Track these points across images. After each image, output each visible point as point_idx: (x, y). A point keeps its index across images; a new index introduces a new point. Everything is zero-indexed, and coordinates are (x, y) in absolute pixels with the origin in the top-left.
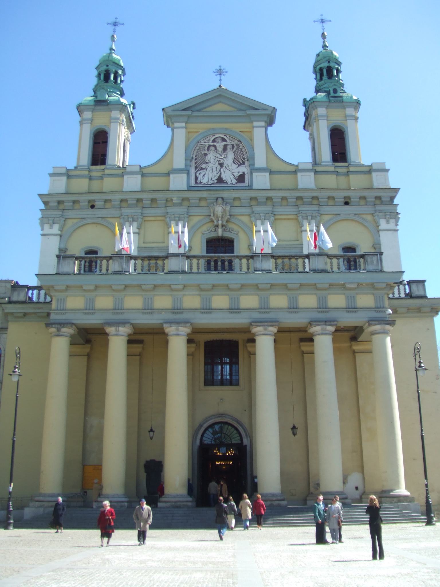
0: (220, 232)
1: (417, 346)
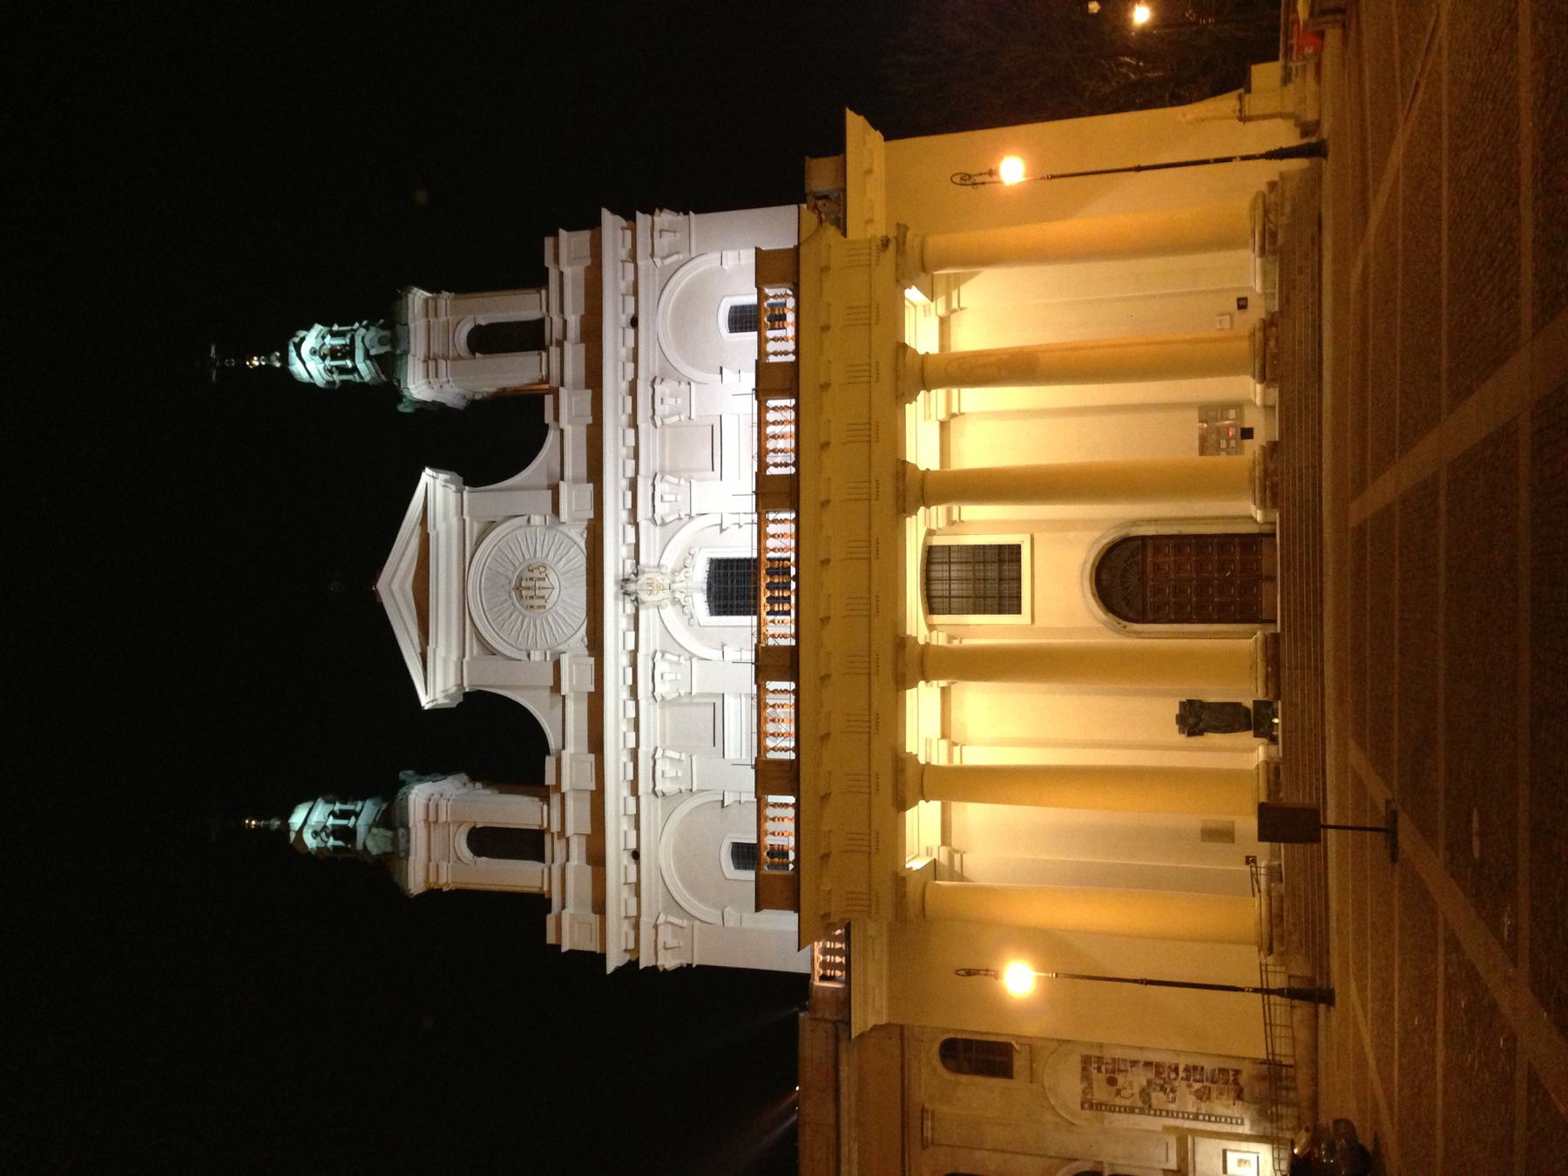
1: (957, 179)
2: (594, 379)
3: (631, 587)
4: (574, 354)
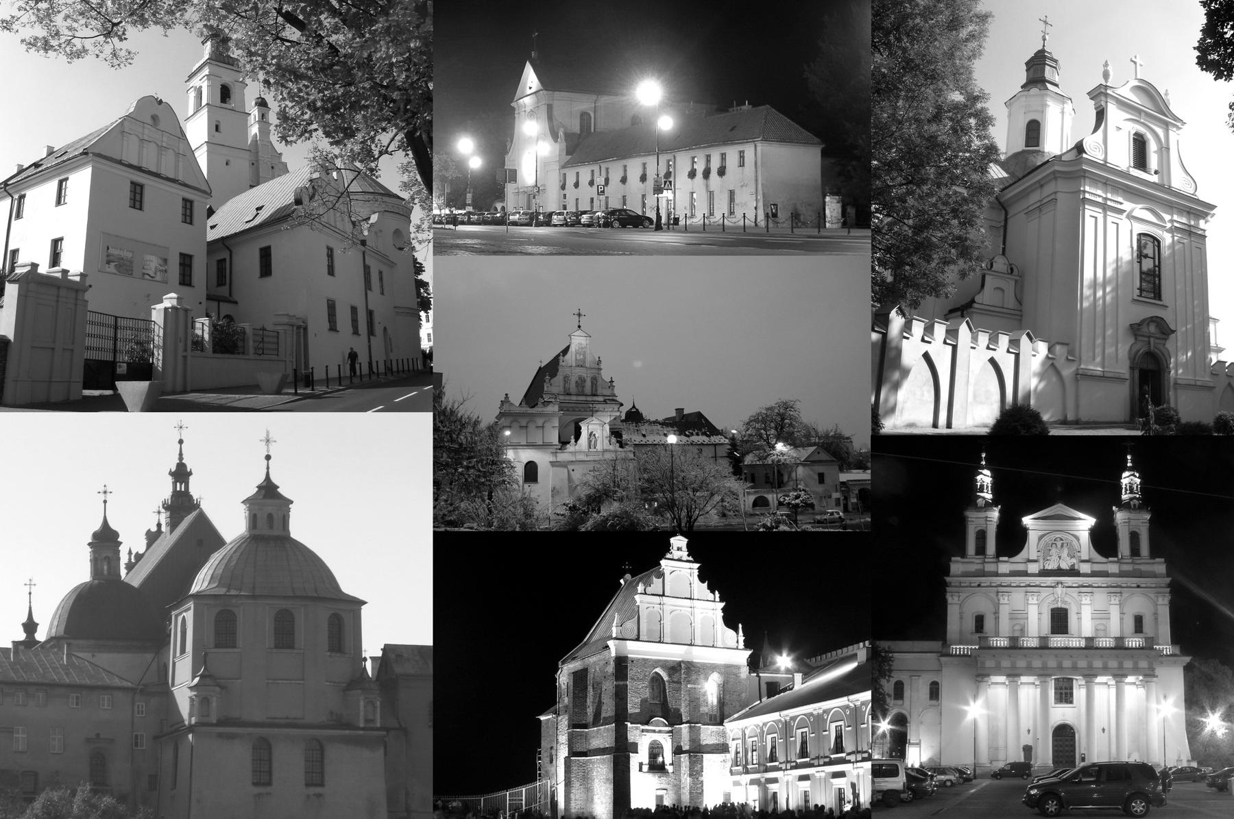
2: (1122, 574)
3: (1060, 585)
4: (1126, 568)
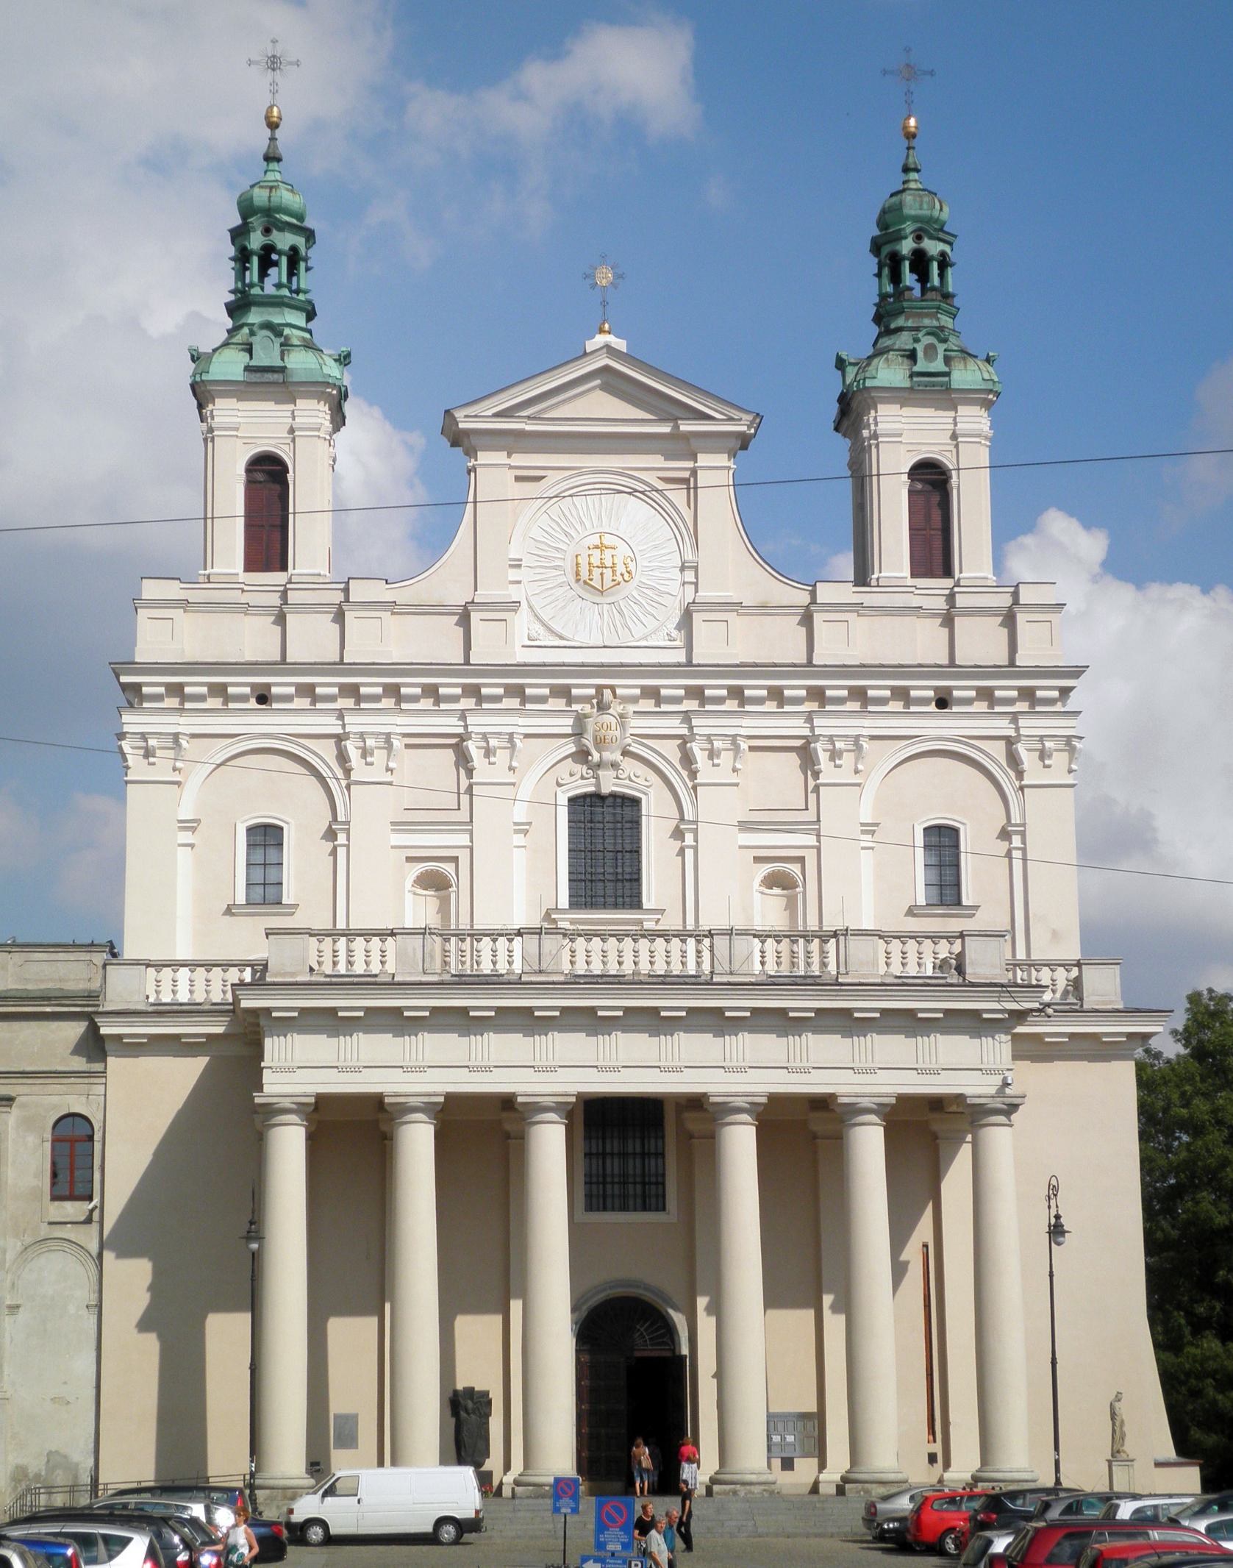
0: (609, 785)
1: (1054, 1182)
